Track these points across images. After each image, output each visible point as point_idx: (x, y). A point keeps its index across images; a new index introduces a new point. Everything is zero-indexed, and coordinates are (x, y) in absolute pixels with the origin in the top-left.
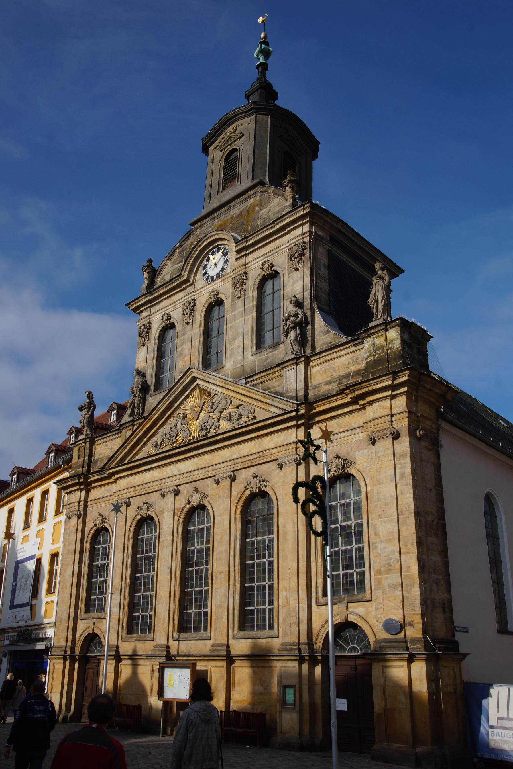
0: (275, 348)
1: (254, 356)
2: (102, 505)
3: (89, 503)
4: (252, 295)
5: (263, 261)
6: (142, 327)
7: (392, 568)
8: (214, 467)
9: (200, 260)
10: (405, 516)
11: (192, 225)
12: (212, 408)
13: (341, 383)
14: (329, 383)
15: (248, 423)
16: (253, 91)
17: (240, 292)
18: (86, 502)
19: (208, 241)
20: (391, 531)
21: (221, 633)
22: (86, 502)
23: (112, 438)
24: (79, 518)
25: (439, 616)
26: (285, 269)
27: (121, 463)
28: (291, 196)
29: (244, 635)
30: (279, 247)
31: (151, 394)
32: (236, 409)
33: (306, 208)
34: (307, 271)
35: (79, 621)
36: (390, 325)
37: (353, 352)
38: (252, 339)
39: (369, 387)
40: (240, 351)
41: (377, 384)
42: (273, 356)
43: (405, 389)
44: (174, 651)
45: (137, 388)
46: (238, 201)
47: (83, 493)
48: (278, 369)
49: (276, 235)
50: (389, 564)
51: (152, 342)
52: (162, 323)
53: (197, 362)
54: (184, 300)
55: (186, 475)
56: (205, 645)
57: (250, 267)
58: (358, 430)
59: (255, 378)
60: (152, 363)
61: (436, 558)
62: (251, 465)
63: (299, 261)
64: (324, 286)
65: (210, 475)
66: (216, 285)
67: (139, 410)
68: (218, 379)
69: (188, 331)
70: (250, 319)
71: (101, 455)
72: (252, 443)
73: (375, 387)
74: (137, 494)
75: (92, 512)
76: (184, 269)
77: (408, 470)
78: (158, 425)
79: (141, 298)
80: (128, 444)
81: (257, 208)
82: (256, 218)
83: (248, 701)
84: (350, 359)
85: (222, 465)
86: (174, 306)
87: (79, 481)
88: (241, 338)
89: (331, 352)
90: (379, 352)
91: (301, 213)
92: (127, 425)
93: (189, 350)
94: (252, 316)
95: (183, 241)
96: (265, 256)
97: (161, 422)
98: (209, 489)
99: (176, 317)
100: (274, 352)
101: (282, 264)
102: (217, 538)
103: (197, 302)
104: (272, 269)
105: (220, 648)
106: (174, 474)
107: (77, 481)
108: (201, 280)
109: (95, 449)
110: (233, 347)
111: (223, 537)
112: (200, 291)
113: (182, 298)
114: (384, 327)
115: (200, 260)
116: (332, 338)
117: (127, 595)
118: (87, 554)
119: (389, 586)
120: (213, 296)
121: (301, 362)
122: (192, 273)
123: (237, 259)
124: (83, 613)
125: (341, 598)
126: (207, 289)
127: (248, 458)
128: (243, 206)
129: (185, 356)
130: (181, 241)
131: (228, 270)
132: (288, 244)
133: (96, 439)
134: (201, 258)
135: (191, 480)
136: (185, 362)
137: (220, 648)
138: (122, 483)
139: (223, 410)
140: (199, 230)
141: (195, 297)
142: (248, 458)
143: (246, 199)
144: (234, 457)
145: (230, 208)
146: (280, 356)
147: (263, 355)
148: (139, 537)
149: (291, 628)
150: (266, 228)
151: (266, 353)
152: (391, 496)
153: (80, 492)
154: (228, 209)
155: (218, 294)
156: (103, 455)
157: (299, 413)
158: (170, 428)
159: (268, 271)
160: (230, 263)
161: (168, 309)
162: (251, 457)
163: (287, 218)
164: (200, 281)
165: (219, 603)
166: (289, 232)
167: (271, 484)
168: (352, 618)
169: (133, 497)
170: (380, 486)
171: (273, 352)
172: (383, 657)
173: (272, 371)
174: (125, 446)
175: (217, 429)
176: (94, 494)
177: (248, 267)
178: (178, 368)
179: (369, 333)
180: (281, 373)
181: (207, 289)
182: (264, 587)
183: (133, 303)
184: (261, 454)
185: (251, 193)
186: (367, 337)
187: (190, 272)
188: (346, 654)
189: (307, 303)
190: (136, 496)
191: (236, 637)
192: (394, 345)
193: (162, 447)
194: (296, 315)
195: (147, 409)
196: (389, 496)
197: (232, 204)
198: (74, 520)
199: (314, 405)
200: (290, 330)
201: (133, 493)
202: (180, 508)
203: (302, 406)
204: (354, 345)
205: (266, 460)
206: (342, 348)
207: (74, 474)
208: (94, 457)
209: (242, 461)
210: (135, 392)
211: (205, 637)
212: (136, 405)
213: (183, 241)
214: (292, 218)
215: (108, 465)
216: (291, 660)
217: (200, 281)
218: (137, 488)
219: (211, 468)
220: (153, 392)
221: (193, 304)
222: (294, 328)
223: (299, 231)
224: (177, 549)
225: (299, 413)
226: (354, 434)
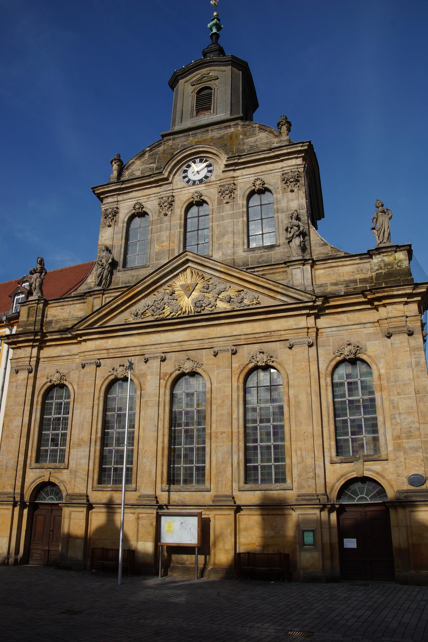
0: (269, 249)
1: (247, 252)
2: (59, 363)
3: (42, 360)
4: (242, 203)
5: (256, 178)
6: (110, 210)
7: (413, 434)
8: (211, 340)
9: (180, 165)
10: (421, 395)
11: (163, 136)
12: (207, 289)
13: (349, 286)
14: (336, 284)
15: (251, 307)
16: (211, 51)
17: (229, 198)
18: (38, 359)
19: (193, 151)
20: (410, 405)
21: (224, 485)
22: (38, 359)
23: (71, 303)
24: (30, 372)
26: (278, 188)
27: (91, 326)
28: (286, 133)
29: (252, 487)
30: (272, 170)
31: (119, 269)
33: (304, 146)
35: (28, 470)
36: (399, 248)
37: (358, 264)
38: (243, 238)
39: (389, 292)
40: (230, 246)
41: (398, 291)
42: (268, 255)
43: (419, 298)
44: (163, 501)
45: (107, 261)
46: (216, 127)
47: (35, 350)
48: (283, 266)
49: (268, 160)
50: (410, 431)
52: (132, 210)
53: (177, 249)
54: (161, 195)
56: (204, 497)
57: (239, 180)
58: (368, 325)
59: (256, 270)
60: (119, 243)
62: (255, 342)
63: (294, 185)
65: (205, 347)
66: (199, 189)
67: (107, 282)
68: (220, 264)
69: (166, 221)
71: (55, 317)
72: (257, 324)
73: (395, 293)
74: (110, 357)
75: (45, 368)
76: (165, 169)
78: (140, 297)
79: (111, 185)
80: (104, 310)
81: (241, 137)
82: (241, 143)
83: (257, 544)
84: (355, 268)
85: (221, 339)
86: (147, 198)
87: (34, 338)
89: (337, 260)
90: (388, 268)
91: (299, 148)
92: (96, 293)
93: (167, 237)
94: (243, 220)
95: (154, 147)
96: (256, 175)
97: (143, 295)
98: (204, 359)
99: (149, 207)
100: (269, 253)
101: (275, 184)
103: (176, 199)
104: (263, 186)
105: (224, 499)
106: (159, 343)
107: (33, 337)
108: (180, 181)
109: (47, 311)
110: (221, 241)
111: (223, 402)
112: (180, 190)
113: (159, 193)
114: (395, 249)
115: (180, 165)
116: (329, 251)
117: (98, 448)
118: (37, 408)
120: (197, 197)
121: (309, 263)
122: (171, 174)
123: (223, 172)
124: (33, 462)
125: (356, 458)
126: (188, 190)
127: (253, 336)
128: (223, 132)
129: (163, 242)
130: (152, 147)
131: (213, 178)
132: (282, 170)
133: (50, 302)
134: (182, 163)
135: (182, 349)
136: (162, 247)
137: (224, 499)
138: (90, 345)
139: (221, 292)
140: (170, 143)
141: (174, 194)
142: (253, 336)
143: (226, 127)
144: (235, 333)
145: (207, 131)
146: (276, 256)
147: (256, 253)
148: (108, 396)
149: (308, 481)
150: (262, 153)
151: (260, 252)
152: (409, 379)
153: (31, 348)
154: (205, 131)
155: (202, 196)
156: (59, 318)
157: (315, 304)
158: (153, 301)
159: (260, 187)
160: (214, 173)
161: (140, 200)
162: (257, 336)
163: (284, 149)
164: (178, 182)
165: (220, 460)
166: (282, 161)
167: (279, 360)
169: (106, 358)
170: (398, 370)
171: (268, 252)
172: (412, 503)
173: (277, 267)
174: (100, 311)
175: (214, 308)
176: (46, 352)
177: (236, 180)
178: (154, 251)
179: (381, 251)
180: (285, 270)
181: (188, 190)
182: (269, 447)
183: (101, 187)
184: (269, 333)
185: (232, 123)
186: (377, 254)
187: (170, 173)
188: (355, 502)
190: (108, 358)
191: (241, 489)
192: (403, 264)
193: (142, 317)
195: (114, 281)
196: (407, 378)
197: (210, 128)
198: (23, 375)
199: (329, 300)
200: (294, 236)
201: (105, 355)
202: (167, 373)
203: (320, 299)
204: (360, 258)
205: (274, 340)
206: (348, 259)
207: (21, 331)
208: (46, 317)
209: (245, 338)
210: (104, 265)
211: (203, 489)
213: (154, 147)
214: (289, 151)
215: (77, 326)
216: (313, 508)
217: (178, 182)
218: (111, 351)
219: (207, 341)
220: (121, 268)
221: (172, 200)
222: (298, 236)
223: (294, 162)
224: (164, 409)
225: (315, 304)
226: (364, 328)
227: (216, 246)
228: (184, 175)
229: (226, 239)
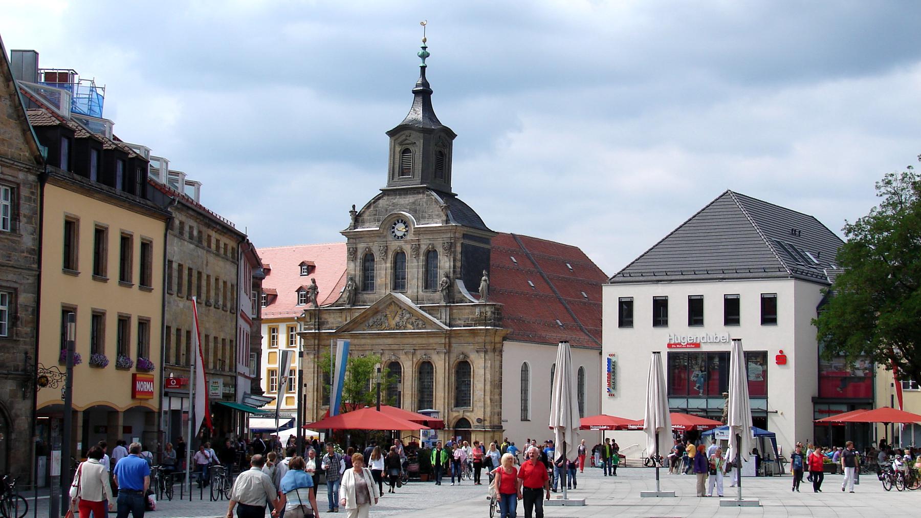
22: (319, 345)
25: (496, 417)
32: (415, 320)
51: (359, 261)
55: (387, 346)
61: (497, 397)
64: (459, 264)
70: (421, 272)
88: (416, 280)
102: (406, 378)
119: (480, 407)
136: (382, 281)
168: (465, 417)
189: (452, 275)
208: (321, 319)
212: (351, 297)
227: (409, 285)
228: (393, 230)
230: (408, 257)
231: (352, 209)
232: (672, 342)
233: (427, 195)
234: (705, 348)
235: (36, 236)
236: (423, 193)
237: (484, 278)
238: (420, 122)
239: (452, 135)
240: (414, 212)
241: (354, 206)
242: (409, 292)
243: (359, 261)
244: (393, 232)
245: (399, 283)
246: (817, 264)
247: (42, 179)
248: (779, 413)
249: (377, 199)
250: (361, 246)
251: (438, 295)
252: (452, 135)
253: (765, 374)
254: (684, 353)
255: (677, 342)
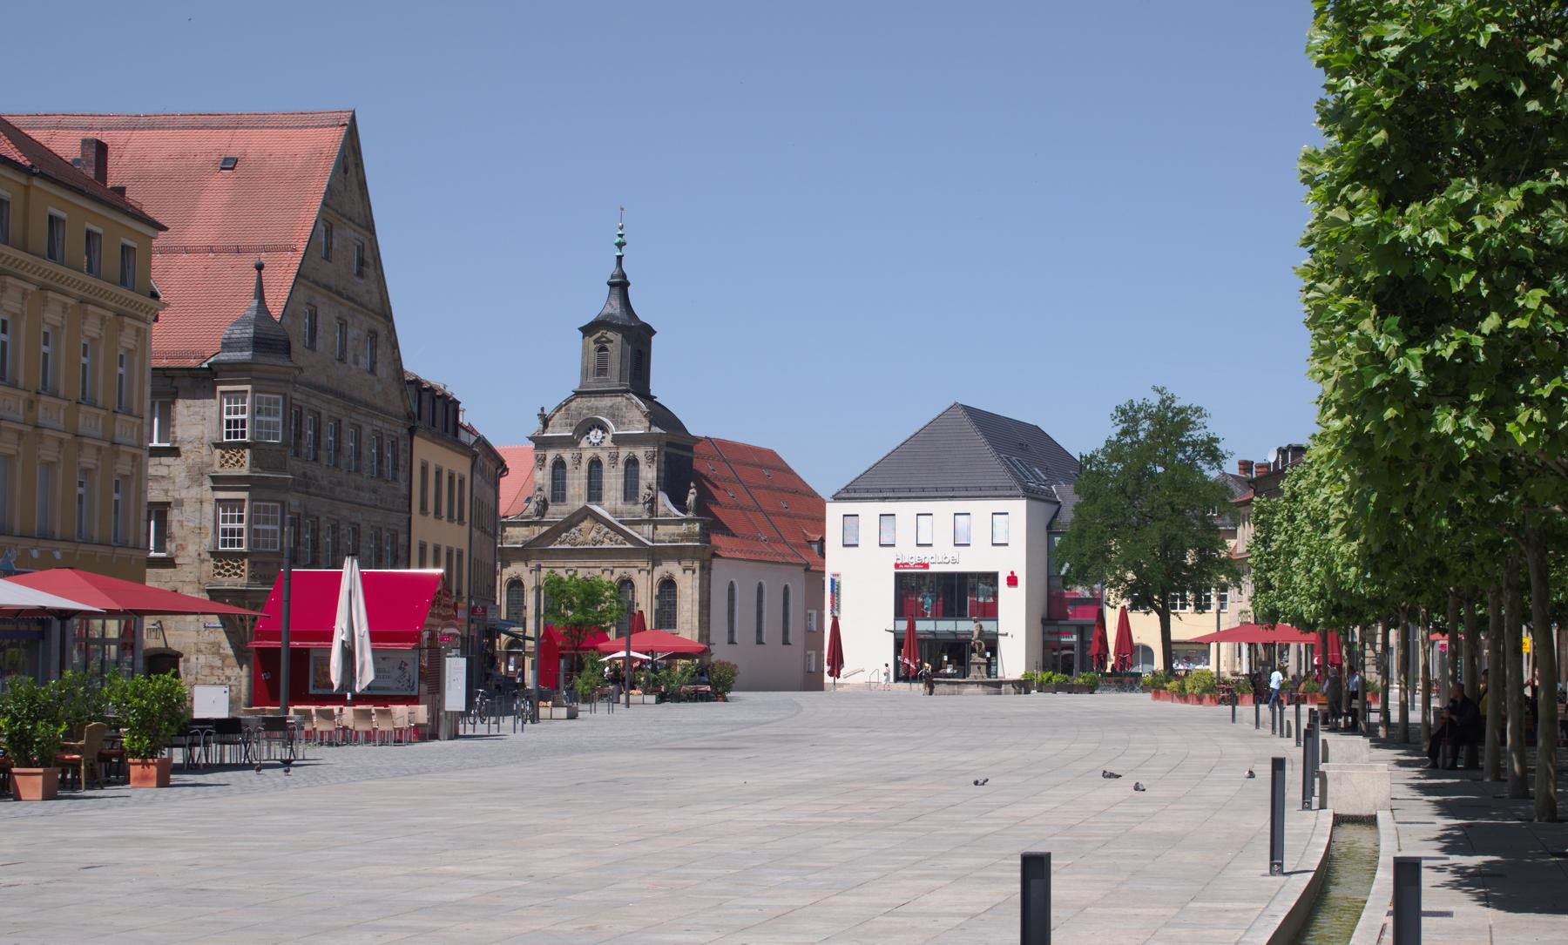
34: (655, 469)
61: (705, 618)
64: (662, 475)
77: (698, 585)
189: (654, 486)
194: (649, 495)
229: (612, 493)
230: (605, 466)
231: (540, 412)
232: (899, 562)
233: (627, 399)
234: (933, 569)
235: (408, 483)
236: (622, 396)
237: (691, 491)
238: (618, 318)
239: (654, 332)
240: (613, 416)
241: (542, 409)
242: (606, 504)
243: (548, 468)
244: (588, 438)
245: (595, 492)
246: (1045, 481)
247: (412, 432)
248: (1009, 635)
249: (569, 401)
250: (551, 455)
251: (639, 508)
252: (654, 332)
253: (995, 595)
254: (912, 574)
255: (904, 562)
